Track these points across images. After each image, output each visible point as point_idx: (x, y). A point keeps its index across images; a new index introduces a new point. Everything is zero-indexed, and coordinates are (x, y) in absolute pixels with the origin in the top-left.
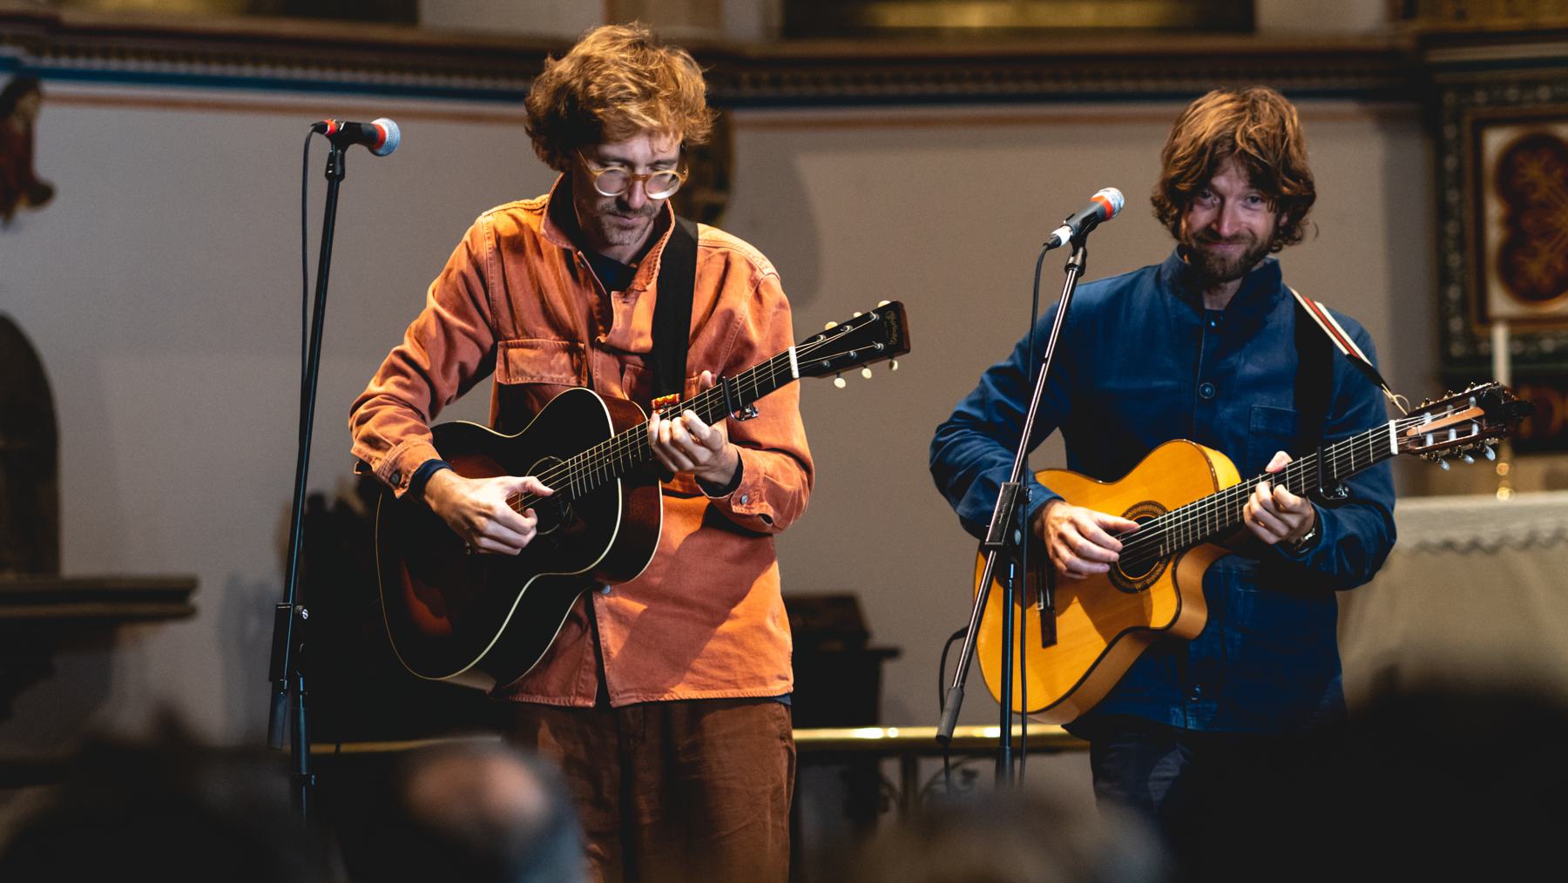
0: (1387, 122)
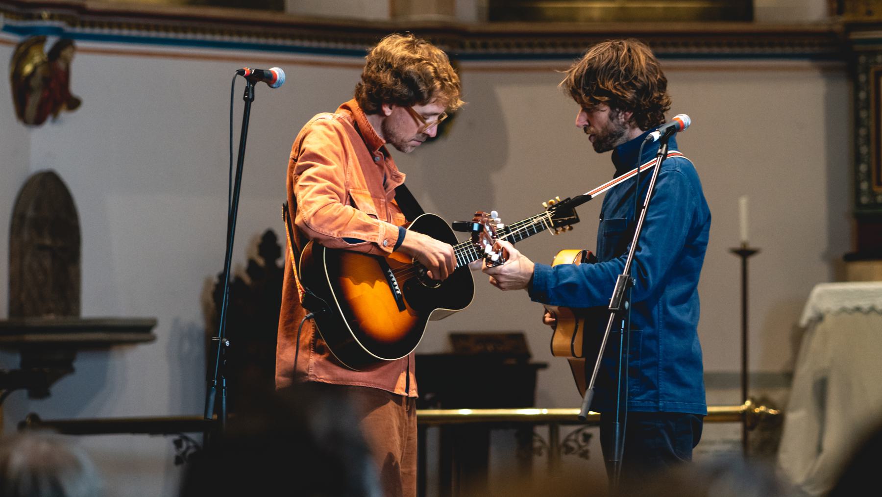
0: (826, 71)
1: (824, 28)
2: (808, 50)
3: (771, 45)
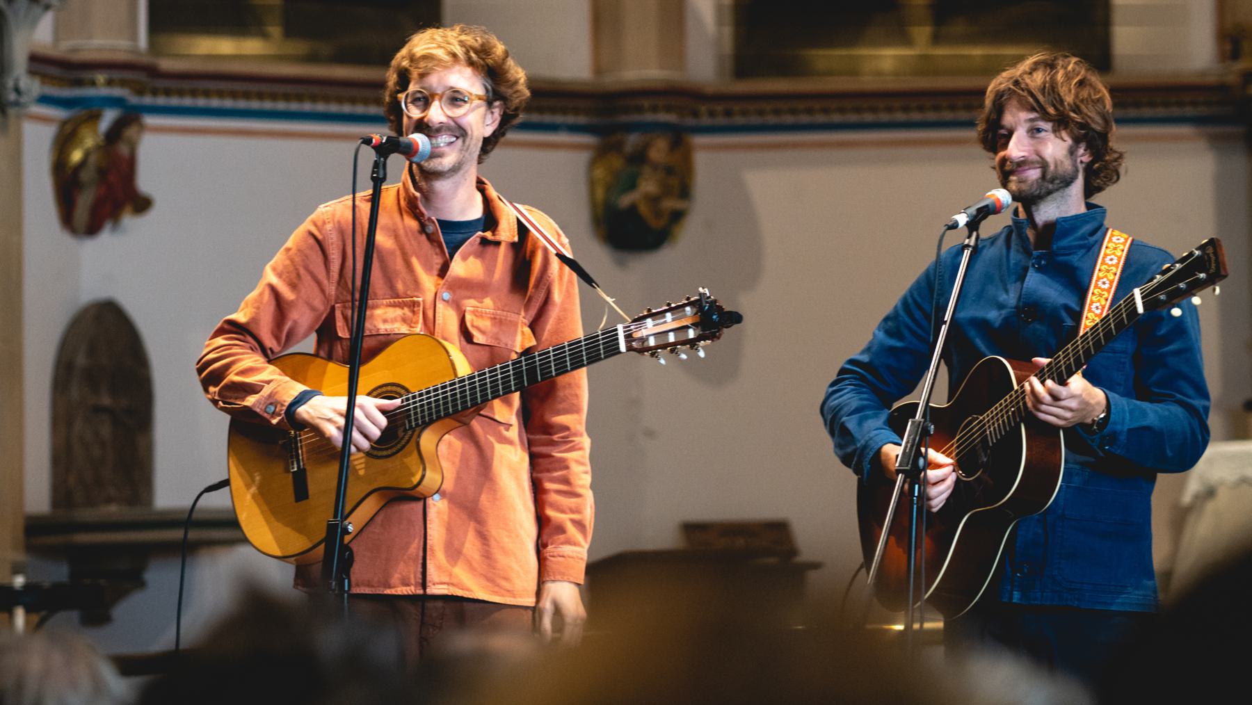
0: (1217, 142)
1: (1211, 80)
2: (1189, 111)
3: (1138, 105)
